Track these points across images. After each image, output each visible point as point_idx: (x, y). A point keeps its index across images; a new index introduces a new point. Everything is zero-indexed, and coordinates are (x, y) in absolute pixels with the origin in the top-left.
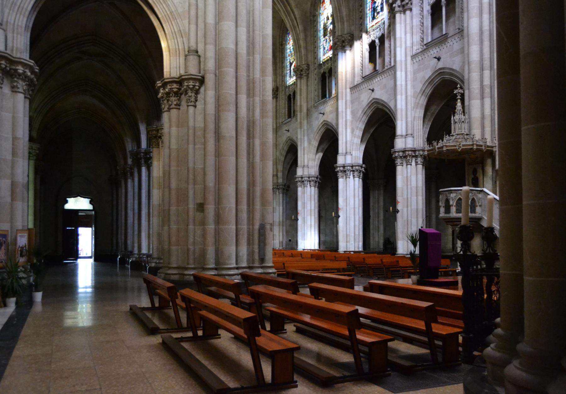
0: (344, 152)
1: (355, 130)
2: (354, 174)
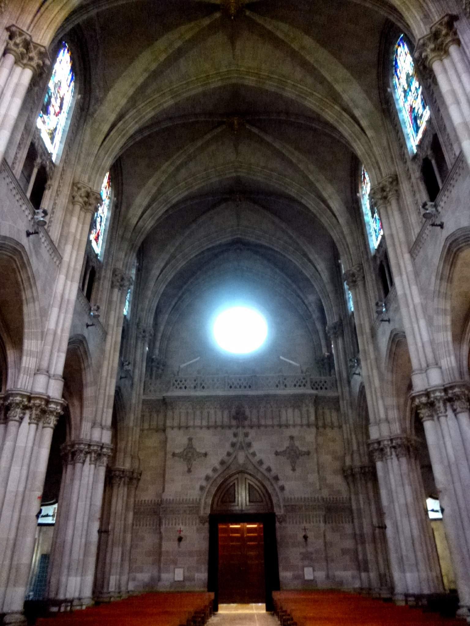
0: (424, 365)
1: (435, 316)
2: (455, 407)
